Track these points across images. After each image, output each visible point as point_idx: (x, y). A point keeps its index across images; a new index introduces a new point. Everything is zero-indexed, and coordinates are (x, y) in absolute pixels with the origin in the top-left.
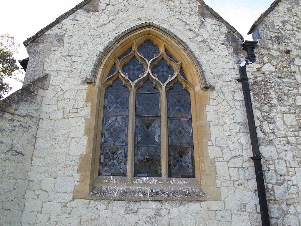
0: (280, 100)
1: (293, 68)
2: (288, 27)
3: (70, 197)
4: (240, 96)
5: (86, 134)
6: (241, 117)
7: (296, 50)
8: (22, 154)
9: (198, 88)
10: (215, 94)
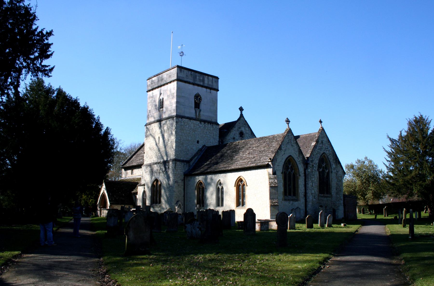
3: (282, 200)
6: (304, 183)
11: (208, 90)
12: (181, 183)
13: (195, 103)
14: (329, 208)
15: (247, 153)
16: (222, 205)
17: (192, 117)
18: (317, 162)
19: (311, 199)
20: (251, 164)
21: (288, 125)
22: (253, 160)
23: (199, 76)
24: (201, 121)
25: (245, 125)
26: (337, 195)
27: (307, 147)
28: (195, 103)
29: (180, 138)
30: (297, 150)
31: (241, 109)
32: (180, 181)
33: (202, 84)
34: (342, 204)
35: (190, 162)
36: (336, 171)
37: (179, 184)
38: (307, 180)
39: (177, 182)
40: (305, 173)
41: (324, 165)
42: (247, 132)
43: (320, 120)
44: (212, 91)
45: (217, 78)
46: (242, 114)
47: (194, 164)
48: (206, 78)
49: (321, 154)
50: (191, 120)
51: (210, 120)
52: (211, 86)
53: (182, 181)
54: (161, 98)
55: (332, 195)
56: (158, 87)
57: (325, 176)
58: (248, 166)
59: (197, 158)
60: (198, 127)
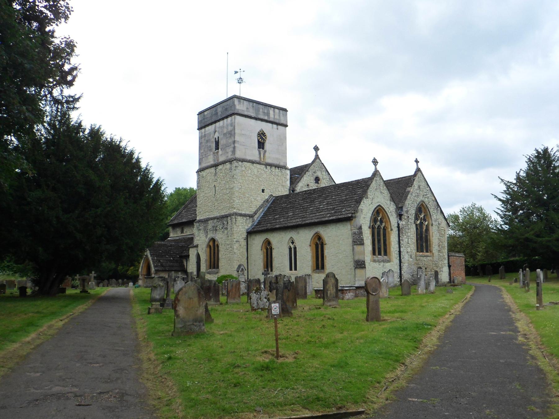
4: (397, 232)
6: (397, 239)
9: (390, 230)
11: (275, 126)
12: (244, 243)
13: (259, 141)
14: (430, 270)
15: (324, 204)
16: (296, 269)
17: (255, 160)
18: (414, 212)
19: (407, 259)
20: (330, 217)
21: (374, 166)
22: (333, 211)
23: (263, 109)
24: (267, 165)
25: (321, 168)
26: (440, 254)
27: (400, 194)
28: (258, 142)
29: (240, 187)
30: (387, 198)
31: (316, 149)
32: (243, 240)
33: (266, 118)
34: (447, 265)
35: (255, 216)
36: (437, 223)
37: (241, 243)
38: (401, 235)
39: (239, 241)
40: (398, 227)
41: (422, 216)
42: (325, 177)
43: (416, 159)
44: (279, 127)
45: (285, 110)
46: (318, 155)
47: (259, 219)
48: (271, 111)
50: (254, 164)
51: (278, 163)
52: (277, 121)
53: (245, 240)
54: (216, 135)
55: (433, 254)
56: (211, 124)
57: (424, 230)
58: (327, 219)
59: (263, 211)
60: (263, 172)
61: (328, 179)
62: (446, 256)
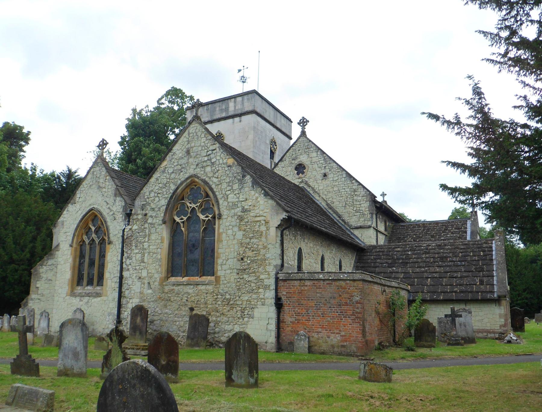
0: (136, 247)
1: (146, 225)
2: (152, 194)
3: (65, 295)
5: (70, 269)
7: (151, 212)
8: (52, 280)
10: (112, 246)
11: (237, 119)
33: (224, 115)
44: (244, 118)
49: (179, 182)
52: (240, 112)
55: (218, 279)
61: (323, 162)
62: (272, 281)
